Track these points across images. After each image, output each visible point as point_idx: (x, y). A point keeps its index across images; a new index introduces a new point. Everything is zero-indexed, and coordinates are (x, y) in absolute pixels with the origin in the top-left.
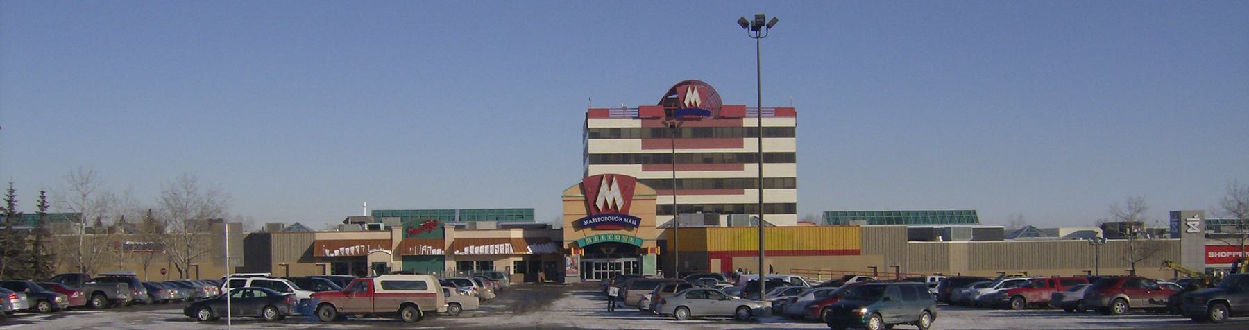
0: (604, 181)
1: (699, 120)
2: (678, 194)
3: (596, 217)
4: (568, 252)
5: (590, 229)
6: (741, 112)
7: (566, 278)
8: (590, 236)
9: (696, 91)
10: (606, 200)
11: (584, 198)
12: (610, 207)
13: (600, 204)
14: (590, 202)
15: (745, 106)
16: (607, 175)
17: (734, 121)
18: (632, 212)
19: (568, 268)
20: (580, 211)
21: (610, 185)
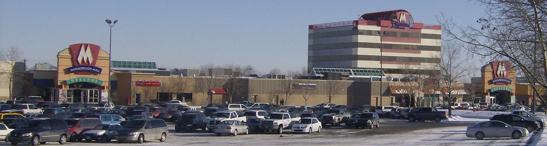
0: (83, 47)
1: (404, 29)
2: (383, 63)
3: (77, 67)
4: (61, 87)
5: (73, 74)
6: (420, 26)
7: (58, 102)
8: (73, 78)
9: (404, 15)
10: (83, 58)
11: (71, 57)
12: (85, 62)
13: (80, 60)
14: (74, 59)
15: (423, 24)
16: (84, 44)
17: (418, 30)
18: (97, 65)
19: (60, 96)
20: (68, 63)
21: (86, 50)
